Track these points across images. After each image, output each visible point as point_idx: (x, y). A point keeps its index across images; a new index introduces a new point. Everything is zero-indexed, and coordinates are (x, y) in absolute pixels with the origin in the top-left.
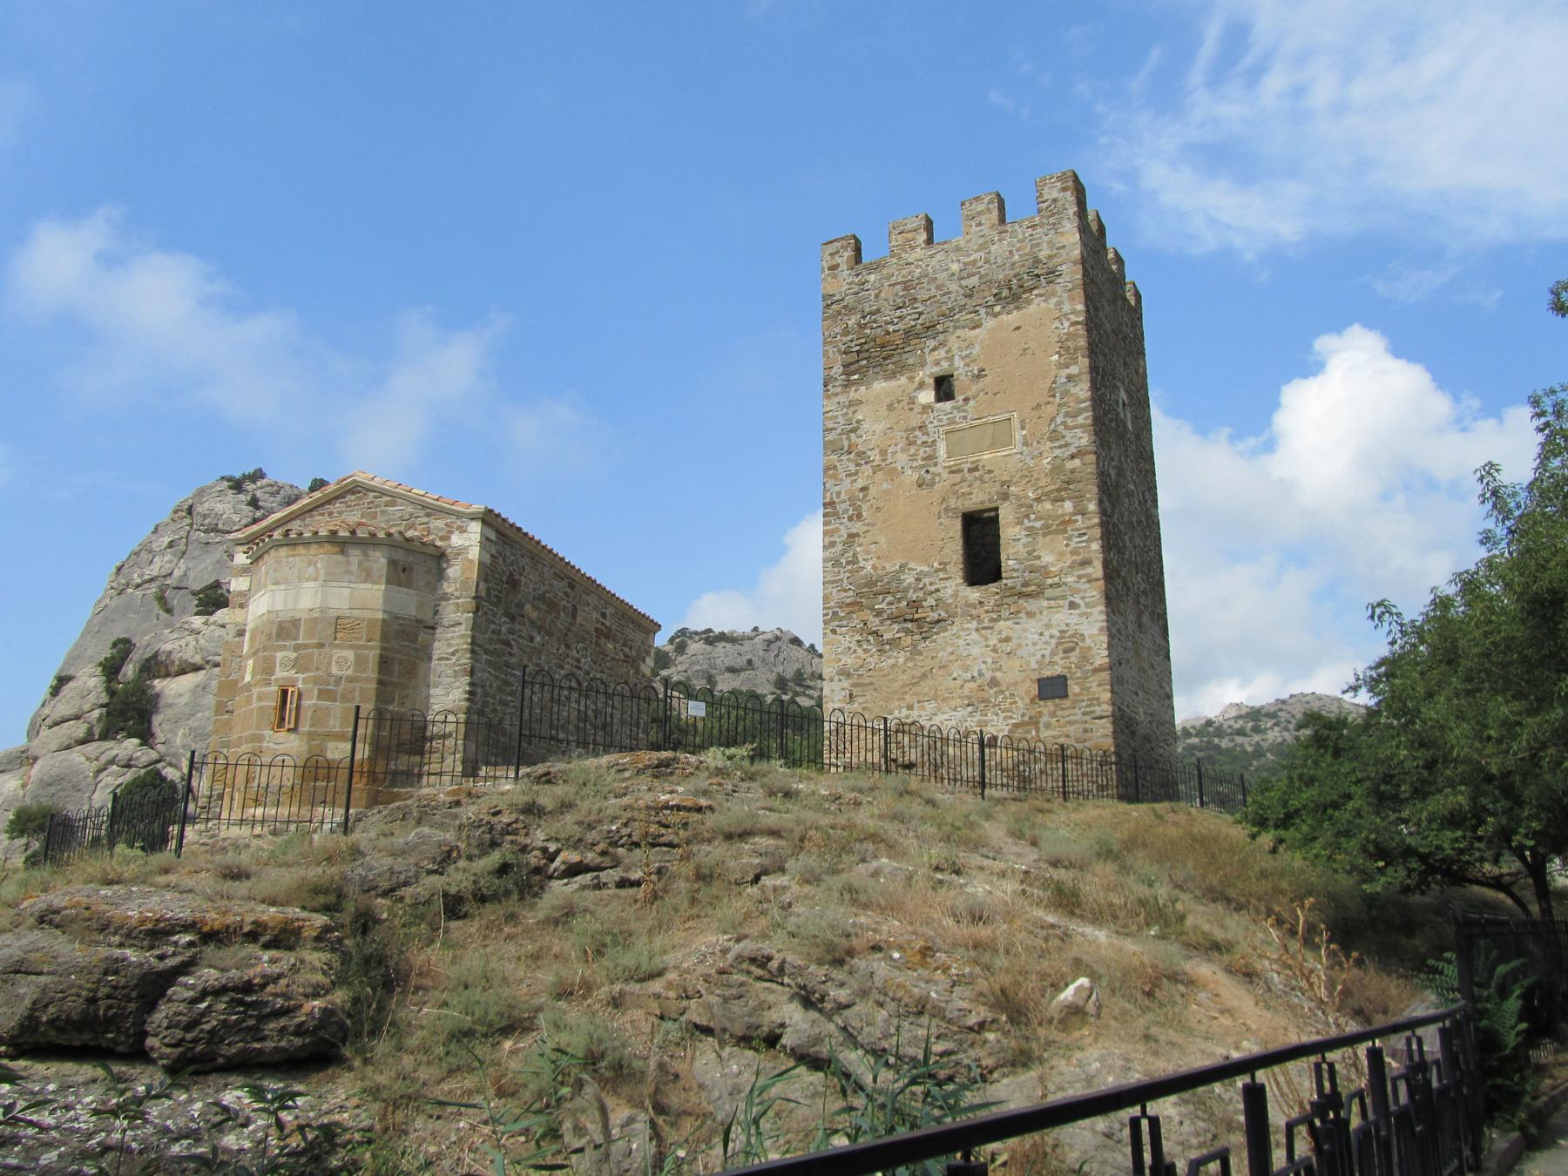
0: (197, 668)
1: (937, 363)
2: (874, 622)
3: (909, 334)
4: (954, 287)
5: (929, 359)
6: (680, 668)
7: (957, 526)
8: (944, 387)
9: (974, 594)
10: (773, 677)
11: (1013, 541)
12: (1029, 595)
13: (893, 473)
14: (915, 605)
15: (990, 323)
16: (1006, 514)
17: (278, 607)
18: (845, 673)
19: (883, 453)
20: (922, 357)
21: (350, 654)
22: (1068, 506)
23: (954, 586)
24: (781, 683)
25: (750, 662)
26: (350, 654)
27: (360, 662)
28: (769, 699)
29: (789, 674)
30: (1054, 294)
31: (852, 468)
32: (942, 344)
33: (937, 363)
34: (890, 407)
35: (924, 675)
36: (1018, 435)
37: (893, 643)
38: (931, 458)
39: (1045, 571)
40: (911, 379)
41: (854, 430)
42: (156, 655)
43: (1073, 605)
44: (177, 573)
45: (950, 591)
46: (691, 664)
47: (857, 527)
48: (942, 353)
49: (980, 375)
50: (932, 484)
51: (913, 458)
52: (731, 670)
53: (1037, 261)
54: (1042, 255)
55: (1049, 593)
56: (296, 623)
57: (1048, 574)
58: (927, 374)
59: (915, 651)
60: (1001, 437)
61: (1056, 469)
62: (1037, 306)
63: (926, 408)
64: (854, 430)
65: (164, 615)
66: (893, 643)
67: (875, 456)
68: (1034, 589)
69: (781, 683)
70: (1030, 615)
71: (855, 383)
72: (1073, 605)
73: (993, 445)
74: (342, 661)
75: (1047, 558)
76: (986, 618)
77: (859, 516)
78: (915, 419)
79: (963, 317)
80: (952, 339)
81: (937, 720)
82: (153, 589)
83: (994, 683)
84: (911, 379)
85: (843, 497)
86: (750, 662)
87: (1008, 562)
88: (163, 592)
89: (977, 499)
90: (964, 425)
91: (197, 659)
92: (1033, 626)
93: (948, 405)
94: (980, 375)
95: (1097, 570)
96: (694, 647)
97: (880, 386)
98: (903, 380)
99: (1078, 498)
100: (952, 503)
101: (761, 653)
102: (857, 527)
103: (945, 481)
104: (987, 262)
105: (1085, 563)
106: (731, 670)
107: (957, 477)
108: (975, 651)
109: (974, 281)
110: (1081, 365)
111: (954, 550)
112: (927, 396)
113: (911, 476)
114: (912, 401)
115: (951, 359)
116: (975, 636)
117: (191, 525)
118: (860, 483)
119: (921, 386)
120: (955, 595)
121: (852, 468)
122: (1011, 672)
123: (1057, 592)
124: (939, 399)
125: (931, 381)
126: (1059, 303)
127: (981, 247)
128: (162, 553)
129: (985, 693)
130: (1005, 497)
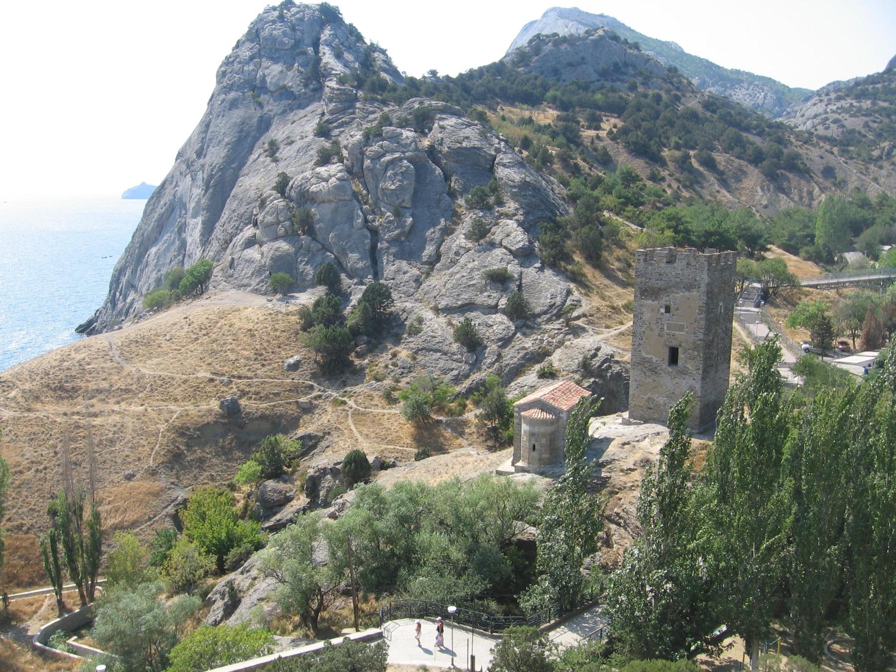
0: (330, 201)
2: (644, 370)
8: (668, 309)
11: (681, 356)
13: (652, 330)
16: (680, 350)
18: (636, 381)
23: (665, 365)
38: (662, 328)
47: (641, 342)
49: (677, 309)
60: (681, 328)
61: (694, 342)
62: (695, 293)
68: (684, 372)
74: (544, 441)
78: (659, 316)
79: (674, 290)
83: (673, 393)
87: (680, 363)
89: (674, 344)
92: (684, 382)
94: (677, 309)
97: (650, 302)
99: (699, 351)
102: (641, 342)
103: (666, 337)
111: (666, 355)
112: (663, 310)
113: (657, 332)
118: (643, 329)
129: (671, 396)
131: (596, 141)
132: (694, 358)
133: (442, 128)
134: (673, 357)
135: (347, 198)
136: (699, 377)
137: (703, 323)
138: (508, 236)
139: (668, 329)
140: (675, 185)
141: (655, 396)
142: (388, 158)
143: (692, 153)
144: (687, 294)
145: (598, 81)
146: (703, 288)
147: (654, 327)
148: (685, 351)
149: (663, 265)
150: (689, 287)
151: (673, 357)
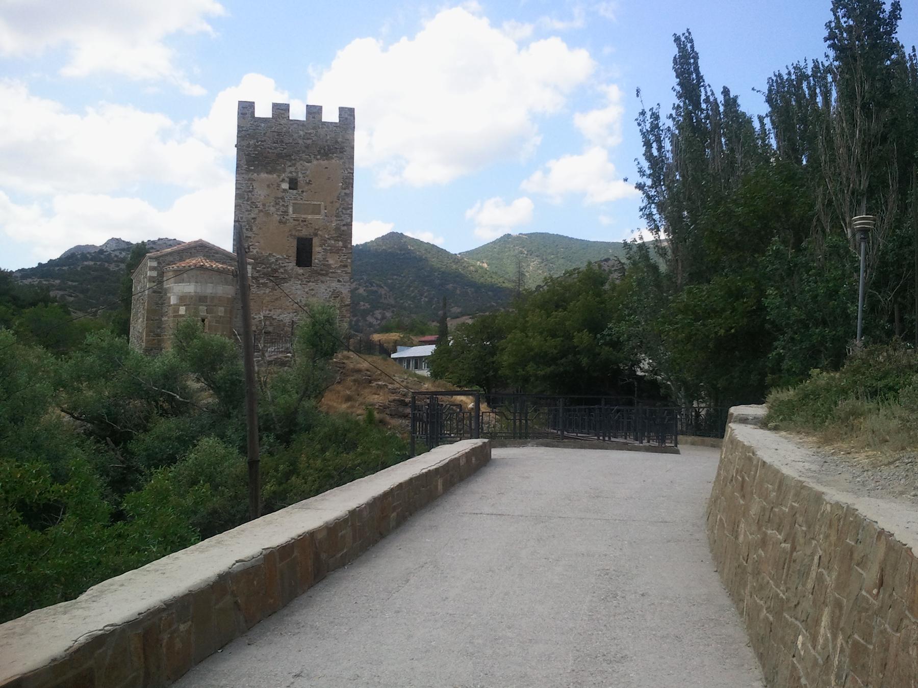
1: (291, 172)
3: (279, 156)
4: (300, 142)
5: (288, 170)
7: (295, 243)
8: (294, 184)
9: (300, 271)
12: (323, 275)
13: (267, 214)
14: (275, 271)
15: (315, 162)
16: (316, 241)
17: (199, 290)
19: (264, 205)
20: (284, 168)
21: (223, 309)
22: (341, 244)
23: (291, 265)
26: (223, 309)
27: (225, 312)
30: (341, 158)
31: (249, 208)
32: (294, 165)
33: (291, 172)
34: (268, 186)
35: (277, 299)
36: (323, 211)
37: (265, 285)
38: (286, 213)
39: (329, 266)
40: (279, 176)
41: (250, 192)
43: (339, 281)
45: (290, 268)
48: (293, 169)
49: (309, 183)
50: (285, 223)
51: (278, 210)
53: (337, 142)
54: (339, 140)
55: (330, 275)
56: (206, 297)
57: (331, 268)
59: (273, 289)
60: (316, 210)
61: (337, 229)
63: (285, 190)
64: (250, 192)
66: (265, 285)
67: (259, 205)
70: (322, 282)
71: (251, 170)
72: (339, 281)
73: (313, 213)
75: (331, 262)
76: (305, 280)
77: (251, 230)
78: (280, 195)
79: (304, 156)
80: (298, 164)
81: (281, 317)
84: (279, 176)
85: (244, 219)
87: (315, 261)
89: (304, 233)
90: (301, 202)
92: (323, 287)
93: (295, 191)
95: (349, 270)
97: (264, 175)
98: (275, 176)
100: (294, 233)
104: (316, 135)
105: (346, 266)
107: (297, 223)
108: (299, 292)
109: (309, 142)
111: (293, 252)
112: (285, 186)
113: (276, 218)
114: (279, 186)
115: (297, 173)
116: (299, 286)
118: (253, 216)
119: (283, 180)
120: (292, 269)
121: (249, 208)
123: (334, 275)
124: (290, 188)
125: (287, 180)
126: (344, 163)
127: (314, 128)
130: (316, 235)
141: (275, 314)
148: (323, 242)
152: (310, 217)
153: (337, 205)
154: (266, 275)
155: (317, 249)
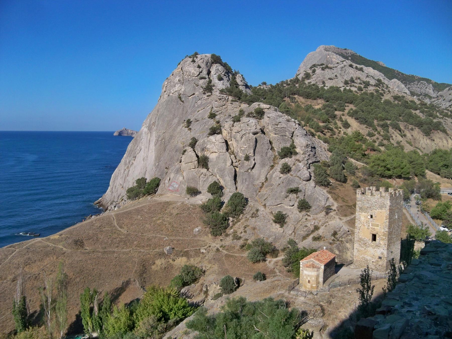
6: (314, 79)
8: (372, 217)
10: (343, 81)
13: (364, 226)
15: (378, 210)
18: (357, 249)
24: (346, 83)
25: (336, 76)
28: (342, 89)
29: (348, 79)
42: (205, 147)
44: (183, 90)
46: (317, 77)
49: (376, 217)
52: (330, 79)
58: (369, 214)
60: (377, 226)
61: (383, 232)
62: (383, 210)
65: (181, 103)
69: (346, 83)
74: (313, 279)
82: (177, 94)
86: (336, 76)
88: (180, 95)
89: (374, 233)
91: (216, 151)
92: (379, 250)
93: (372, 219)
96: (318, 71)
97: (363, 213)
99: (385, 236)
101: (340, 72)
106: (330, 79)
110: (388, 220)
112: (369, 217)
117: (183, 74)
122: (376, 254)
128: (177, 83)
131: (342, 117)
132: (383, 240)
133: (269, 117)
134: (374, 238)
135: (224, 151)
136: (386, 248)
137: (387, 223)
138: (300, 171)
139: (372, 226)
140: (381, 138)
141: (365, 256)
142: (243, 132)
143: (389, 122)
144: (380, 211)
145: (344, 86)
146: (388, 208)
147: (365, 224)
149: (369, 196)
150: (381, 207)
151: (374, 238)
152: (376, 228)
153: (384, 225)
154: (363, 244)
155: (377, 238)
